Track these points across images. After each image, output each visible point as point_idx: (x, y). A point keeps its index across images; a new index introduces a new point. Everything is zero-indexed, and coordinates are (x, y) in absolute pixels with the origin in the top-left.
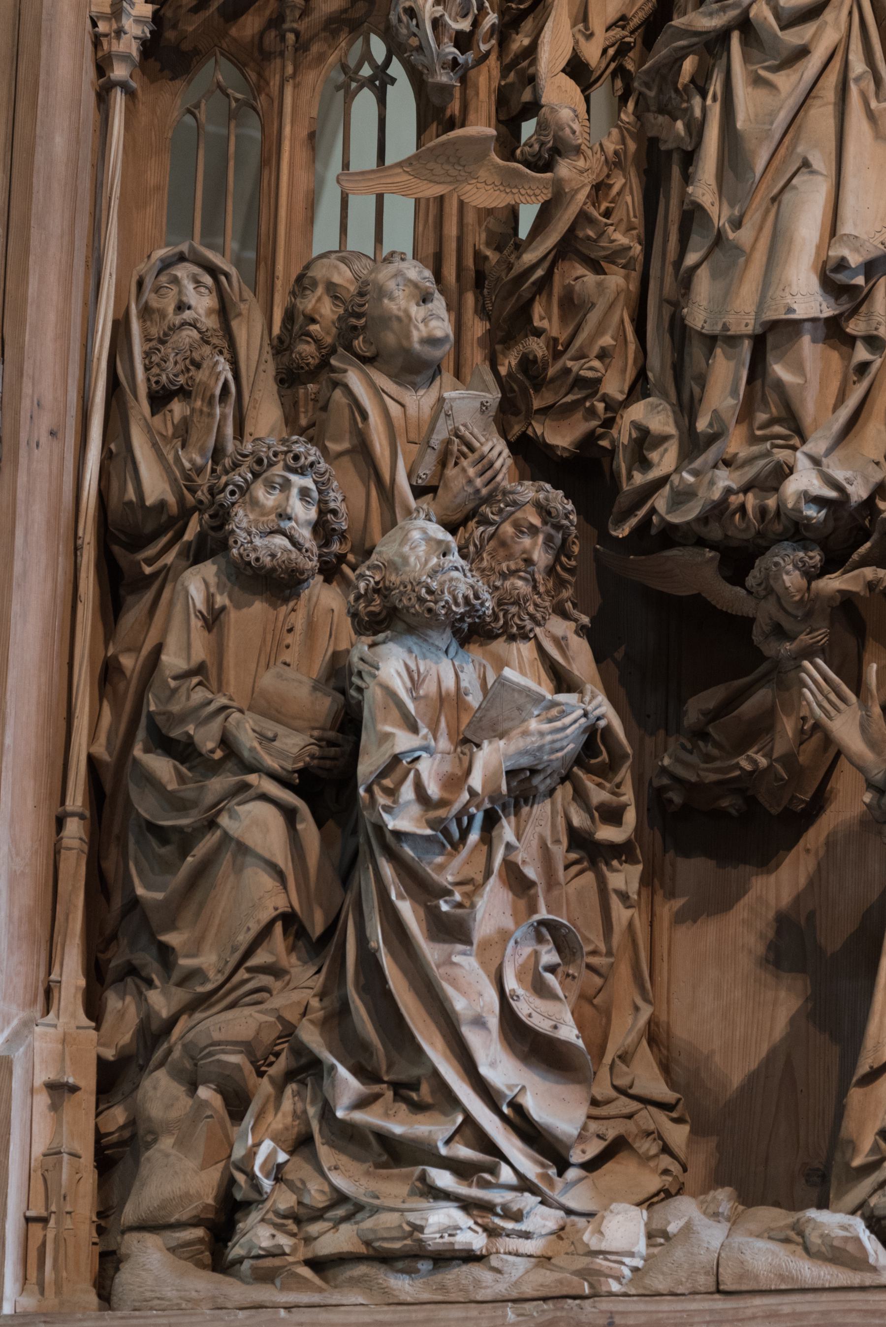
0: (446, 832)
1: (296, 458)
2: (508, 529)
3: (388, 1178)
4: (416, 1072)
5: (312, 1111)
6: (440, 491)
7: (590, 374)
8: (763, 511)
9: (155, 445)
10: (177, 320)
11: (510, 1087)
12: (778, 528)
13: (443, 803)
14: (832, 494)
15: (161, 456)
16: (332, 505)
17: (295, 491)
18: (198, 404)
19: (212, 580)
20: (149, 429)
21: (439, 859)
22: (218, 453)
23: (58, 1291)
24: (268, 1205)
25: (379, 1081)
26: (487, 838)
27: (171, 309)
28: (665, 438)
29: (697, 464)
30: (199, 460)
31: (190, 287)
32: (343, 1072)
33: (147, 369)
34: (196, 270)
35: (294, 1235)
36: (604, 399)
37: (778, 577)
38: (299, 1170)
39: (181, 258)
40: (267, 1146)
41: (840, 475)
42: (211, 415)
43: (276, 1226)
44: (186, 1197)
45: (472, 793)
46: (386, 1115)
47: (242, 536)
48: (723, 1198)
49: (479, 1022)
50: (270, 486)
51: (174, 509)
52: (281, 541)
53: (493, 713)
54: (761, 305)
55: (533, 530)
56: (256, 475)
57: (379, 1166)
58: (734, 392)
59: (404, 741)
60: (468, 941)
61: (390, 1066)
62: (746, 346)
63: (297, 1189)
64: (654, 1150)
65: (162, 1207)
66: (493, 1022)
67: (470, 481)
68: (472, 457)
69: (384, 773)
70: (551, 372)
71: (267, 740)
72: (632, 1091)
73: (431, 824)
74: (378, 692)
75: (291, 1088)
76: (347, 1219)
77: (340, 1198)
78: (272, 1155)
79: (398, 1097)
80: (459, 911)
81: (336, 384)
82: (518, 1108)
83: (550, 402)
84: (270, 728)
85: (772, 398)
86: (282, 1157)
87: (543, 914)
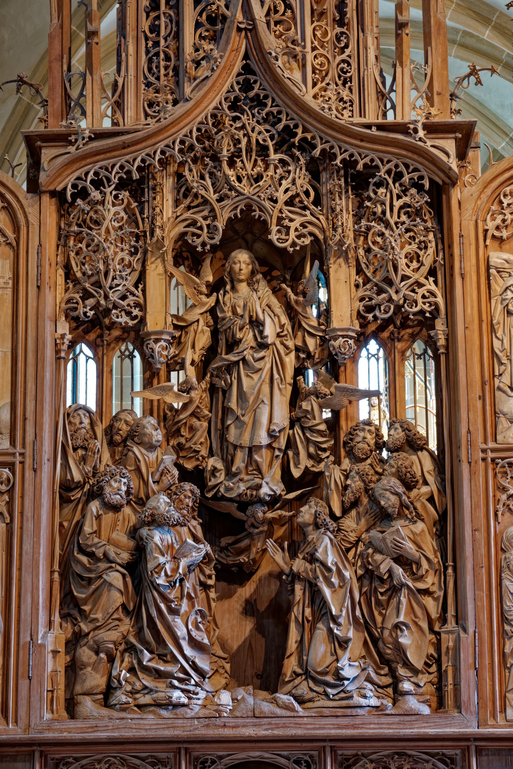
0: (171, 585)
1: (124, 474)
2: (182, 497)
3: (159, 682)
4: (165, 652)
5: (135, 662)
6: (160, 483)
7: (198, 449)
8: (252, 495)
9: (76, 464)
10: (80, 426)
11: (192, 656)
12: (256, 499)
13: (171, 576)
14: (273, 493)
15: (78, 468)
16: (132, 486)
17: (122, 483)
18: (90, 453)
19: (98, 507)
20: (74, 459)
21: (169, 591)
22: (95, 468)
23: (57, 713)
24: (124, 689)
25: (154, 653)
26: (181, 585)
27: (78, 423)
28: (221, 470)
29: (234, 481)
30: (90, 469)
31: (83, 416)
32: (145, 651)
33: (71, 440)
34: (85, 412)
35: (130, 697)
36: (202, 456)
37: (256, 514)
38: (134, 679)
39: (80, 408)
40: (124, 672)
41: (274, 488)
42: (94, 457)
43: (126, 695)
44: (98, 686)
45: (180, 574)
46: (157, 663)
47: (108, 496)
48: (251, 688)
49: (184, 639)
50: (116, 481)
51: (82, 483)
52: (118, 496)
53: (183, 551)
54: (252, 439)
55: (189, 497)
56: (111, 478)
57: (155, 678)
58: (243, 462)
59: (162, 560)
60: (178, 615)
61: (157, 649)
62: (247, 449)
63: (132, 684)
64: (223, 672)
65: (91, 688)
66: (187, 638)
67: (169, 481)
68: (170, 474)
69: (155, 568)
70: (186, 447)
71: (117, 554)
72: (216, 654)
73: (168, 582)
74: (154, 545)
75: (127, 655)
76: (147, 693)
77: (145, 687)
78: (125, 675)
79: (159, 658)
80: (177, 607)
81: (129, 450)
82: (193, 662)
83: (185, 455)
84: (119, 551)
85: (254, 464)
86: (128, 675)
87: (197, 608)
